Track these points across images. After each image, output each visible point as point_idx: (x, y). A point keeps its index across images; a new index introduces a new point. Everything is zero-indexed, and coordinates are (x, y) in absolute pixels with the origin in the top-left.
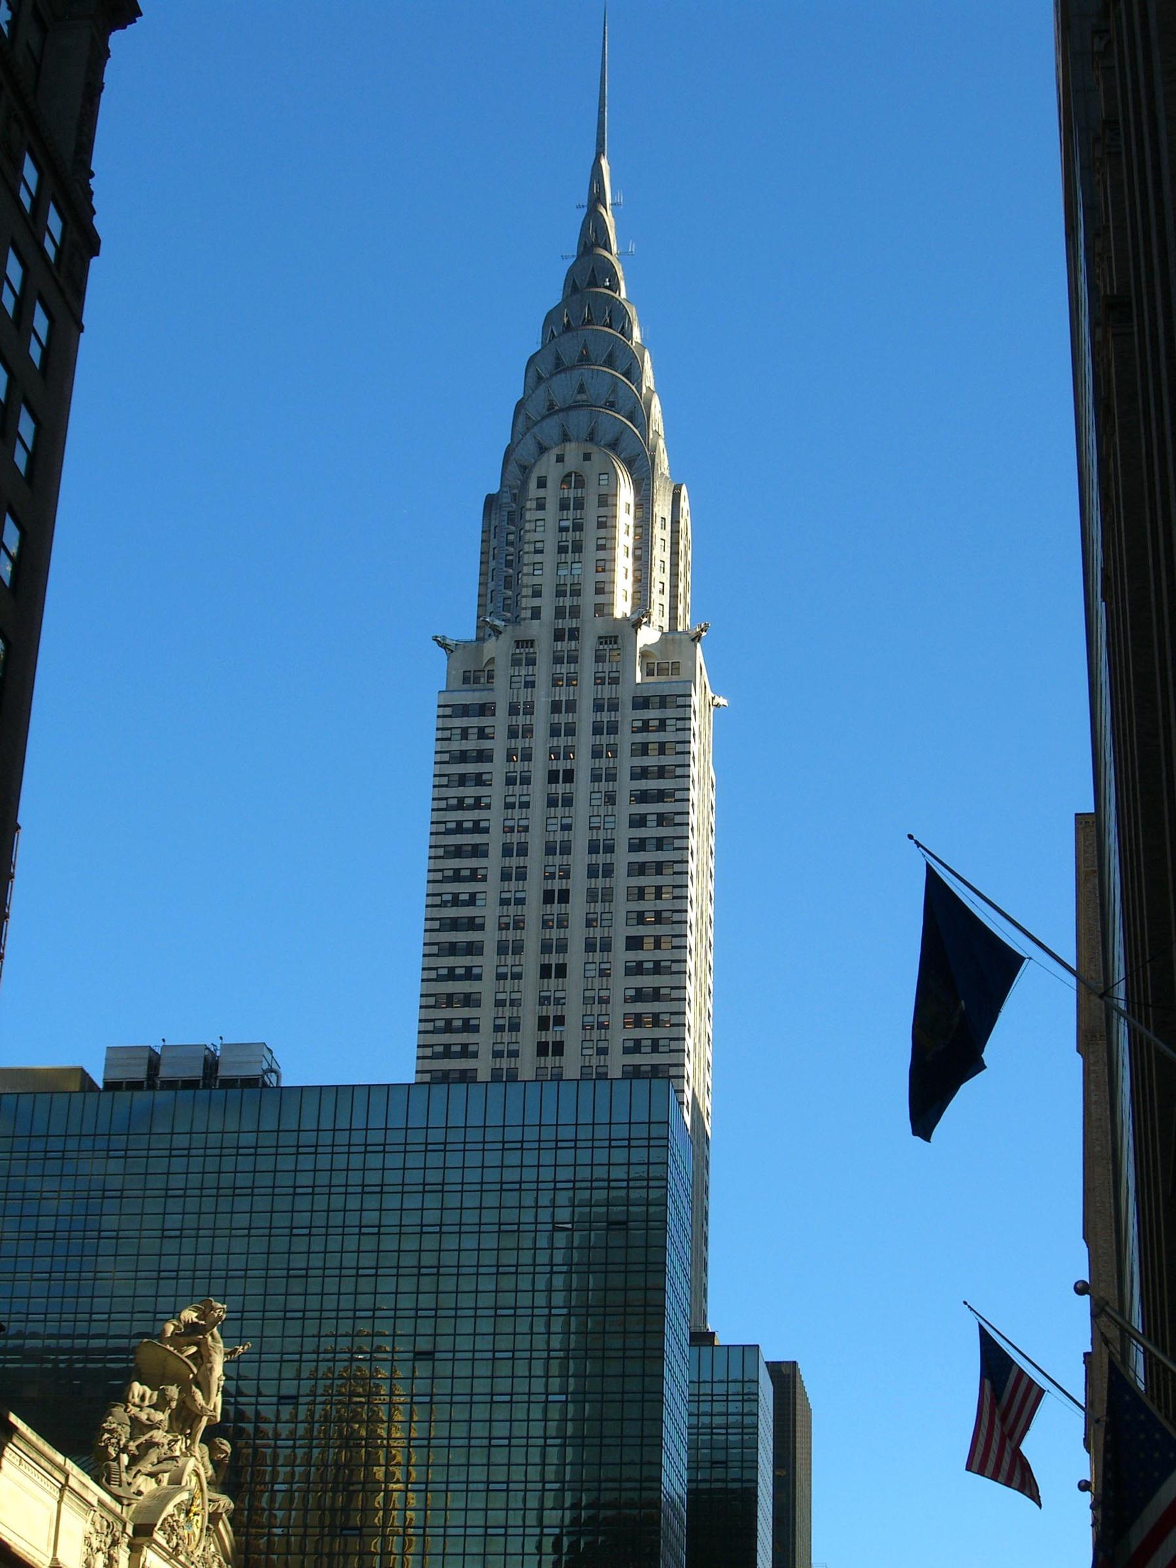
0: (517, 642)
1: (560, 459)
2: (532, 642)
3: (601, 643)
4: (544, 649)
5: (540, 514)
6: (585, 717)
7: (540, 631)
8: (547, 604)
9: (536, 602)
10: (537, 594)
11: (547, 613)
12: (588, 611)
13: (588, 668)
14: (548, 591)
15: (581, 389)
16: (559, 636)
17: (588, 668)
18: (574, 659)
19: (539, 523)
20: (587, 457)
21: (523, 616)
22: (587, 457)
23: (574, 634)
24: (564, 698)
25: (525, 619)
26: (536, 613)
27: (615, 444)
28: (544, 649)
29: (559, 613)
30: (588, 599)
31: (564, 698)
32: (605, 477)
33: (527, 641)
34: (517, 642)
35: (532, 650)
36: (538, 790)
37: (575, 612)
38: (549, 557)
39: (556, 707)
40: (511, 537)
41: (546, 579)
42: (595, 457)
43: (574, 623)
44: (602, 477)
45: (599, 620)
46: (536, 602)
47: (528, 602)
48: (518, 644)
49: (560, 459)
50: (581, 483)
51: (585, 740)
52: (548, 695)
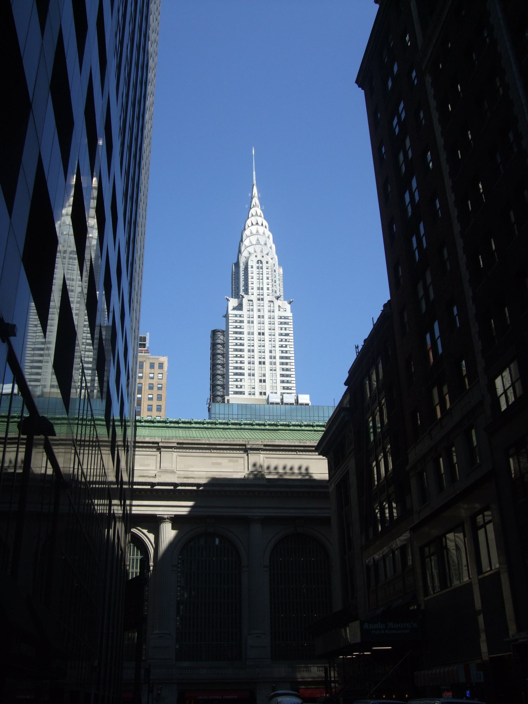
2: (252, 301)
6: (266, 320)
7: (254, 298)
10: (253, 289)
11: (255, 294)
12: (265, 295)
14: (255, 288)
20: (263, 257)
30: (265, 291)
36: (256, 336)
38: (255, 280)
39: (259, 317)
41: (255, 286)
43: (262, 297)
50: (261, 263)
51: (267, 326)
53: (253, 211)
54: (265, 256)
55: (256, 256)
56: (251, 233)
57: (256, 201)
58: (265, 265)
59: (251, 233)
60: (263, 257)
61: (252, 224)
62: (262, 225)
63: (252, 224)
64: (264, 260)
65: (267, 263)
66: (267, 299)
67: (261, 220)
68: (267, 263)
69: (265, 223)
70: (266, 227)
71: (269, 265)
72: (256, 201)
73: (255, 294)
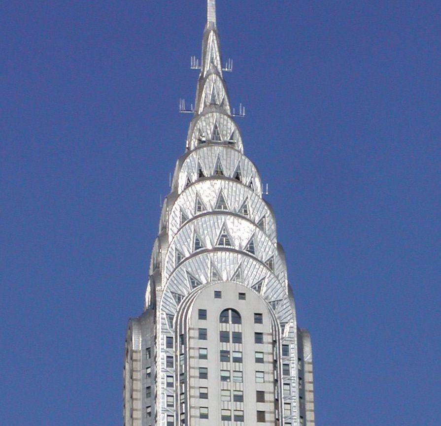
53: (205, 126)
54: (251, 295)
55: (218, 294)
56: (199, 206)
57: (213, 88)
58: (248, 328)
59: (199, 206)
60: (242, 296)
61: (201, 175)
62: (237, 178)
63: (201, 175)
64: (246, 310)
65: (258, 318)
67: (236, 159)
68: (258, 318)
69: (250, 174)
70: (250, 186)
71: (265, 327)
72: (213, 88)
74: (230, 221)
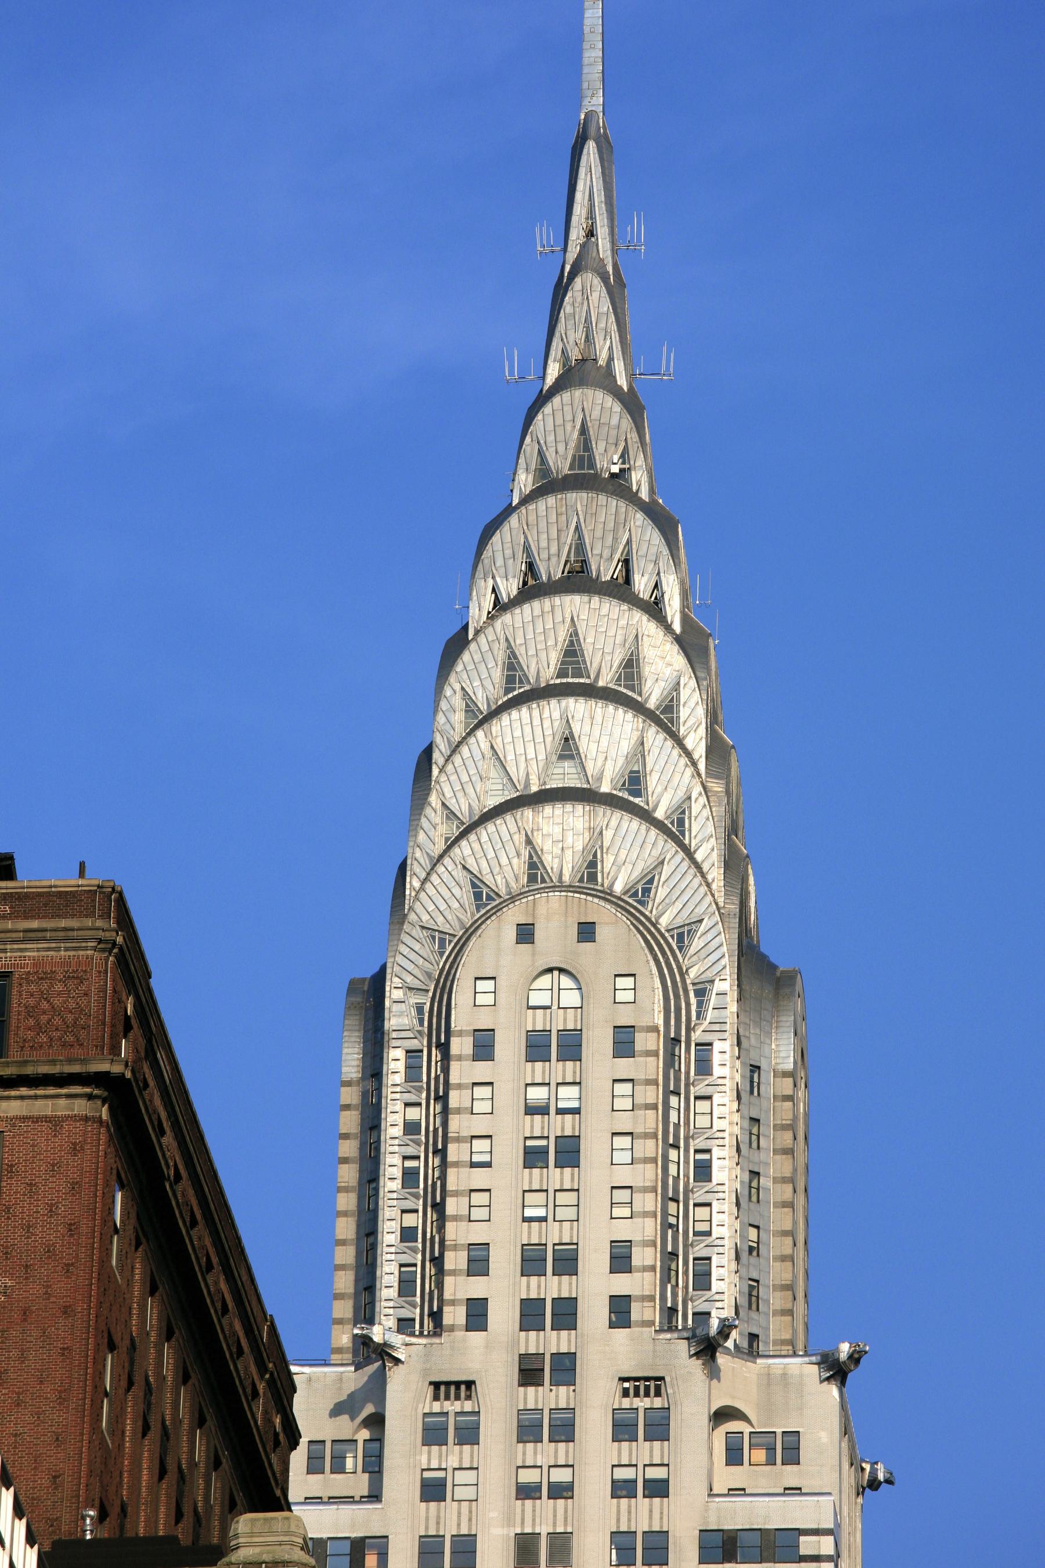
0: (436, 1385)
1: (525, 934)
2: (470, 1384)
3: (626, 1393)
4: (499, 1400)
5: (482, 1070)
7: (488, 1358)
8: (504, 1289)
9: (476, 1287)
10: (479, 1263)
11: (503, 1315)
12: (594, 1313)
13: (596, 1456)
14: (504, 1260)
15: (568, 747)
16: (529, 1373)
17: (596, 1456)
18: (564, 1429)
19: (481, 1092)
20: (587, 932)
21: (447, 1319)
22: (587, 932)
23: (565, 1368)
24: (544, 1530)
25: (452, 1328)
26: (477, 1314)
27: (646, 891)
28: (499, 1400)
29: (531, 1314)
30: (594, 1285)
31: (544, 1530)
32: (628, 982)
33: (458, 1384)
34: (436, 1385)
35: (468, 1406)
37: (566, 1313)
40: (413, 1114)
42: (602, 932)
44: (621, 982)
45: (621, 1333)
46: (476, 1287)
47: (459, 1287)
48: (440, 1388)
49: (525, 934)
52: (509, 1522)
66: (607, 1355)
73: (503, 1315)
74: (577, 707)
